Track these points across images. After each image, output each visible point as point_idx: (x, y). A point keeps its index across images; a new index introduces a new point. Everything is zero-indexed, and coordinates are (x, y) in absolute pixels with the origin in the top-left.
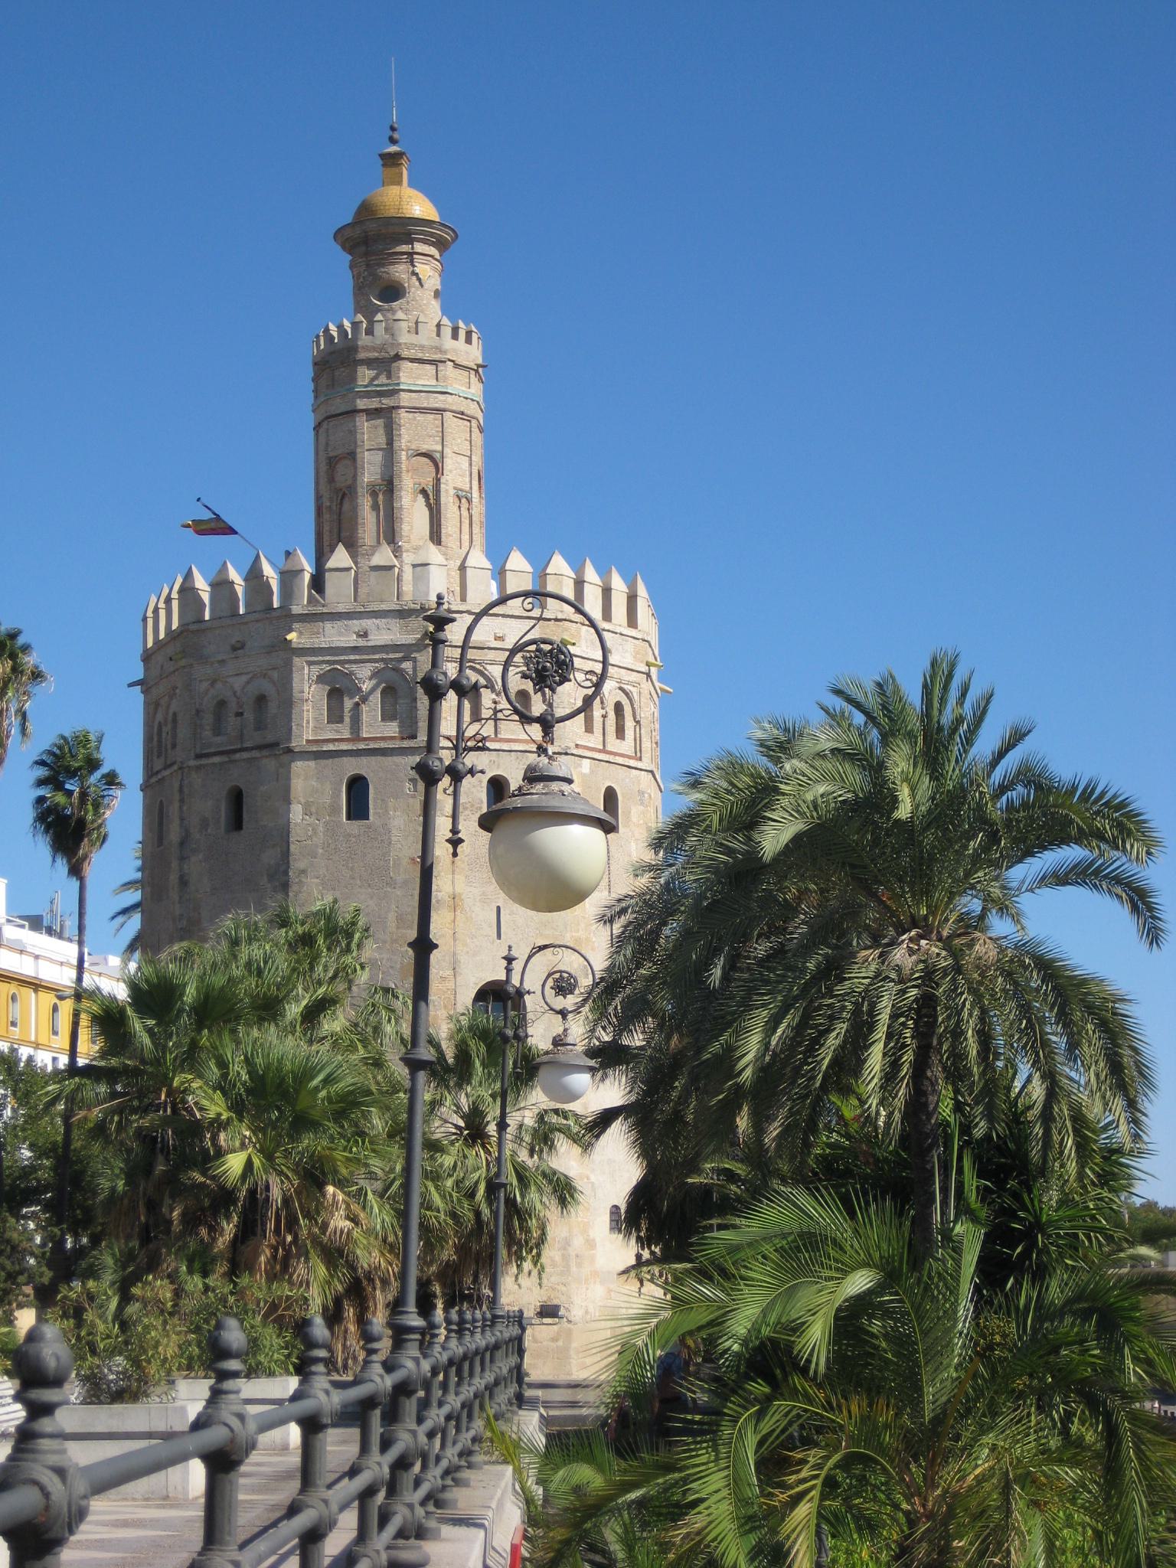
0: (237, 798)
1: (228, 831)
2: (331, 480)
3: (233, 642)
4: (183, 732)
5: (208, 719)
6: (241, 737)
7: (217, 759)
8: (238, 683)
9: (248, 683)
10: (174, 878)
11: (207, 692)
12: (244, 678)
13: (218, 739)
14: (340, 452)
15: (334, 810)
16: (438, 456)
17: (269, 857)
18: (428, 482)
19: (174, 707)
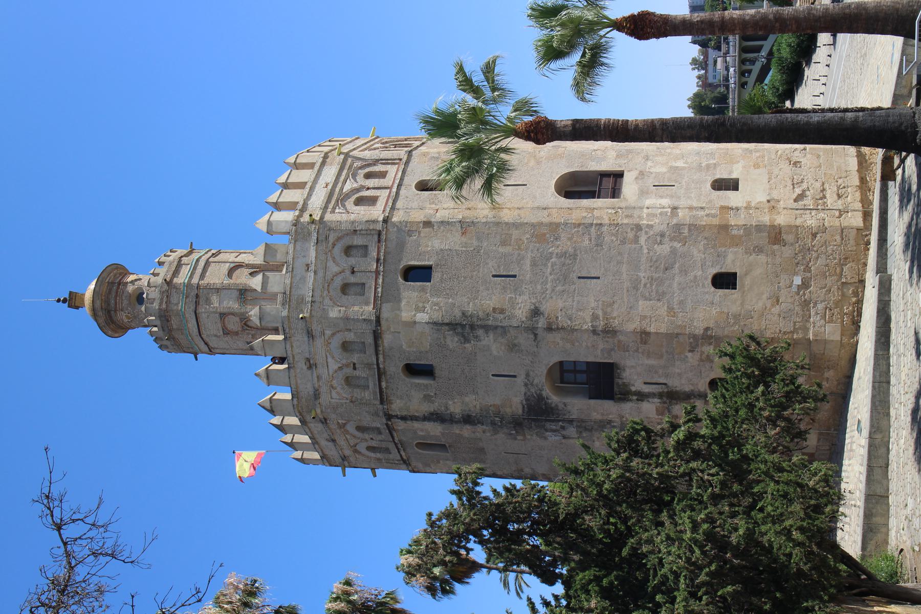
0: (412, 370)
1: (434, 379)
2: (237, 333)
3: (305, 367)
4: (367, 420)
5: (358, 394)
6: (369, 366)
7: (384, 384)
8: (333, 366)
9: (333, 358)
10: (466, 431)
11: (337, 393)
12: (330, 360)
13: (371, 385)
14: (220, 325)
15: (423, 290)
16: (232, 265)
17: (452, 341)
18: (246, 271)
19: (351, 428)
